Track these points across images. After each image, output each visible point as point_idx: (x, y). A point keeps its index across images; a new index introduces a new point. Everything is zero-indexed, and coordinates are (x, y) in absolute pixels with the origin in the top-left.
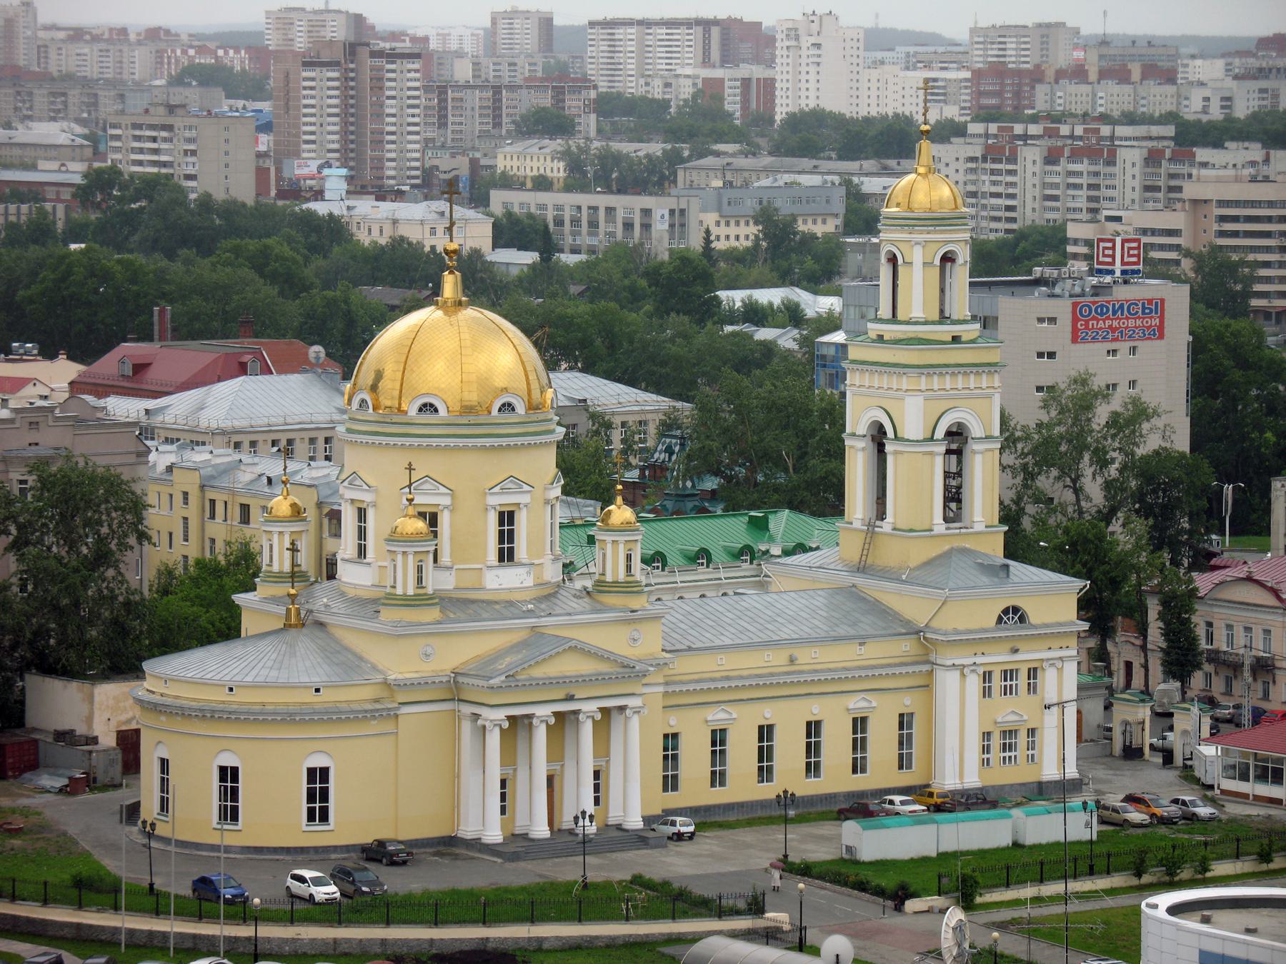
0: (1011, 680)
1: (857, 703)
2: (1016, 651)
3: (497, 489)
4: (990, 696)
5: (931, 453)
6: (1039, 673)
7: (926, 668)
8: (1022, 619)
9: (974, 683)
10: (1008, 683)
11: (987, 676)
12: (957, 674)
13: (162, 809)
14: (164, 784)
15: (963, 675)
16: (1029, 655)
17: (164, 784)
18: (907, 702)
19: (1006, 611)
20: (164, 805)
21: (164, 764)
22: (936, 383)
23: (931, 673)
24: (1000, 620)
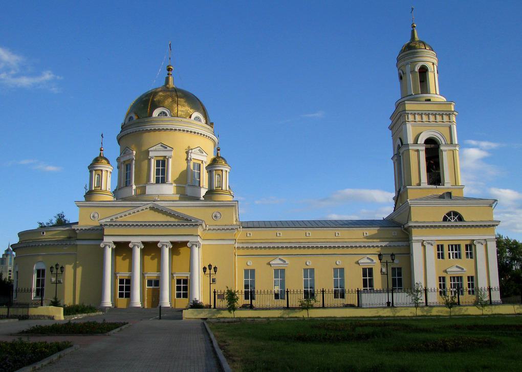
5: (418, 151)
7: (404, 244)
8: (460, 219)
9: (432, 252)
11: (440, 248)
15: (423, 245)
16: (462, 237)
19: (449, 214)
24: (445, 219)
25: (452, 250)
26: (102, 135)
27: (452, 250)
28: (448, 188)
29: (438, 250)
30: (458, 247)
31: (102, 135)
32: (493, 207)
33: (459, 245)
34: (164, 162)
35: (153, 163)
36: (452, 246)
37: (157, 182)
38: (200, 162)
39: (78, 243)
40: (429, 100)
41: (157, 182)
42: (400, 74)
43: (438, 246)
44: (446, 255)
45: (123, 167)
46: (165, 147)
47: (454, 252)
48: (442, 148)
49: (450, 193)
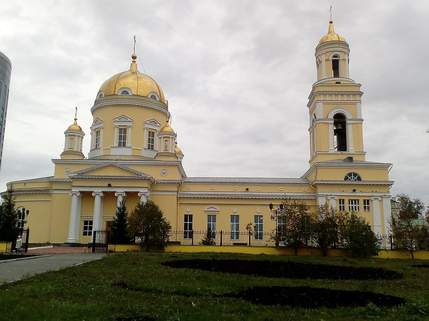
0: (355, 204)
2: (354, 191)
3: (117, 120)
8: (359, 179)
10: (354, 205)
19: (350, 174)
22: (328, 98)
24: (346, 179)
25: (352, 204)
26: (76, 108)
27: (352, 204)
28: (350, 154)
29: (340, 203)
30: (356, 201)
31: (76, 108)
32: (389, 170)
33: (358, 200)
34: (125, 130)
35: (117, 131)
36: (352, 200)
37: (120, 145)
38: (153, 131)
40: (339, 83)
41: (120, 145)
42: (317, 62)
43: (340, 200)
45: (95, 133)
47: (354, 205)
48: (348, 122)
49: (352, 158)
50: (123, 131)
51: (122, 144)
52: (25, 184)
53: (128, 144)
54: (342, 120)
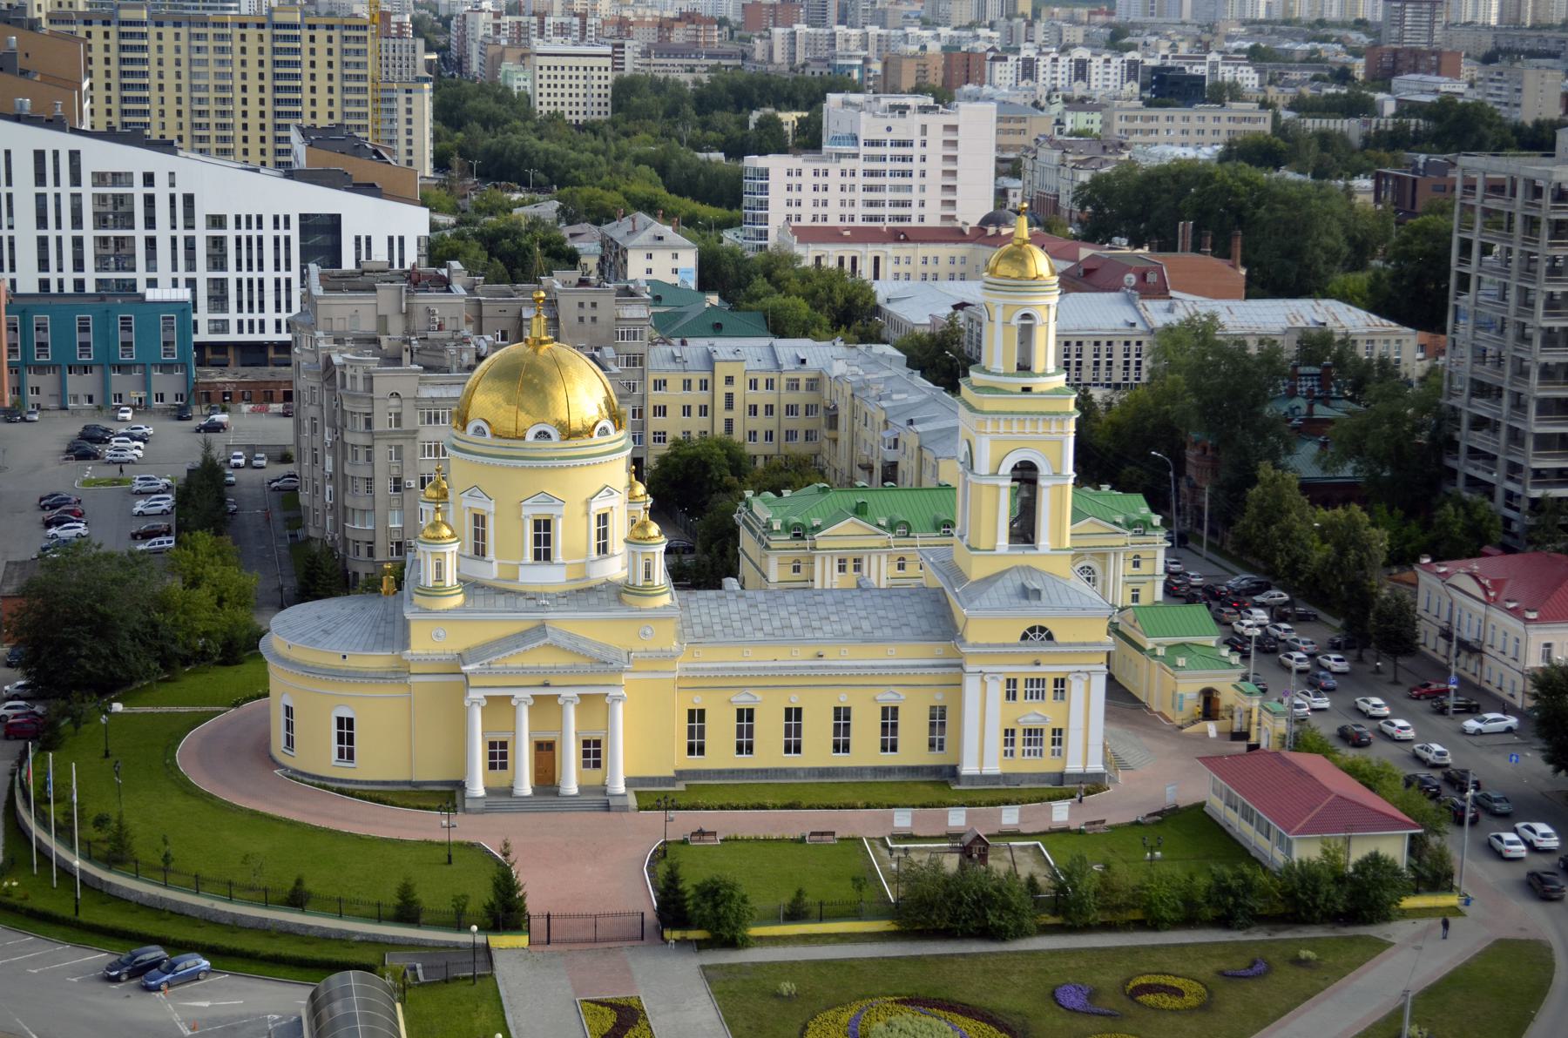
1: (888, 698)
4: (1014, 698)
5: (998, 487)
6: (1066, 683)
8: (1050, 637)
9: (997, 690)
10: (1035, 689)
11: (1011, 683)
12: (977, 679)
13: (288, 744)
14: (289, 726)
15: (982, 680)
17: (289, 726)
18: (938, 698)
19: (1032, 630)
20: (290, 742)
21: (289, 711)
23: (960, 676)
24: (1025, 637)
25: (1032, 686)
27: (1032, 686)
29: (1008, 687)
30: (1040, 682)
34: (547, 524)
36: (1032, 680)
37: (537, 557)
39: (413, 679)
43: (1009, 680)
44: (1020, 694)
46: (551, 499)
47: (1035, 689)
50: (543, 528)
51: (543, 553)
52: (344, 657)
53: (558, 554)
54: (1028, 474)
